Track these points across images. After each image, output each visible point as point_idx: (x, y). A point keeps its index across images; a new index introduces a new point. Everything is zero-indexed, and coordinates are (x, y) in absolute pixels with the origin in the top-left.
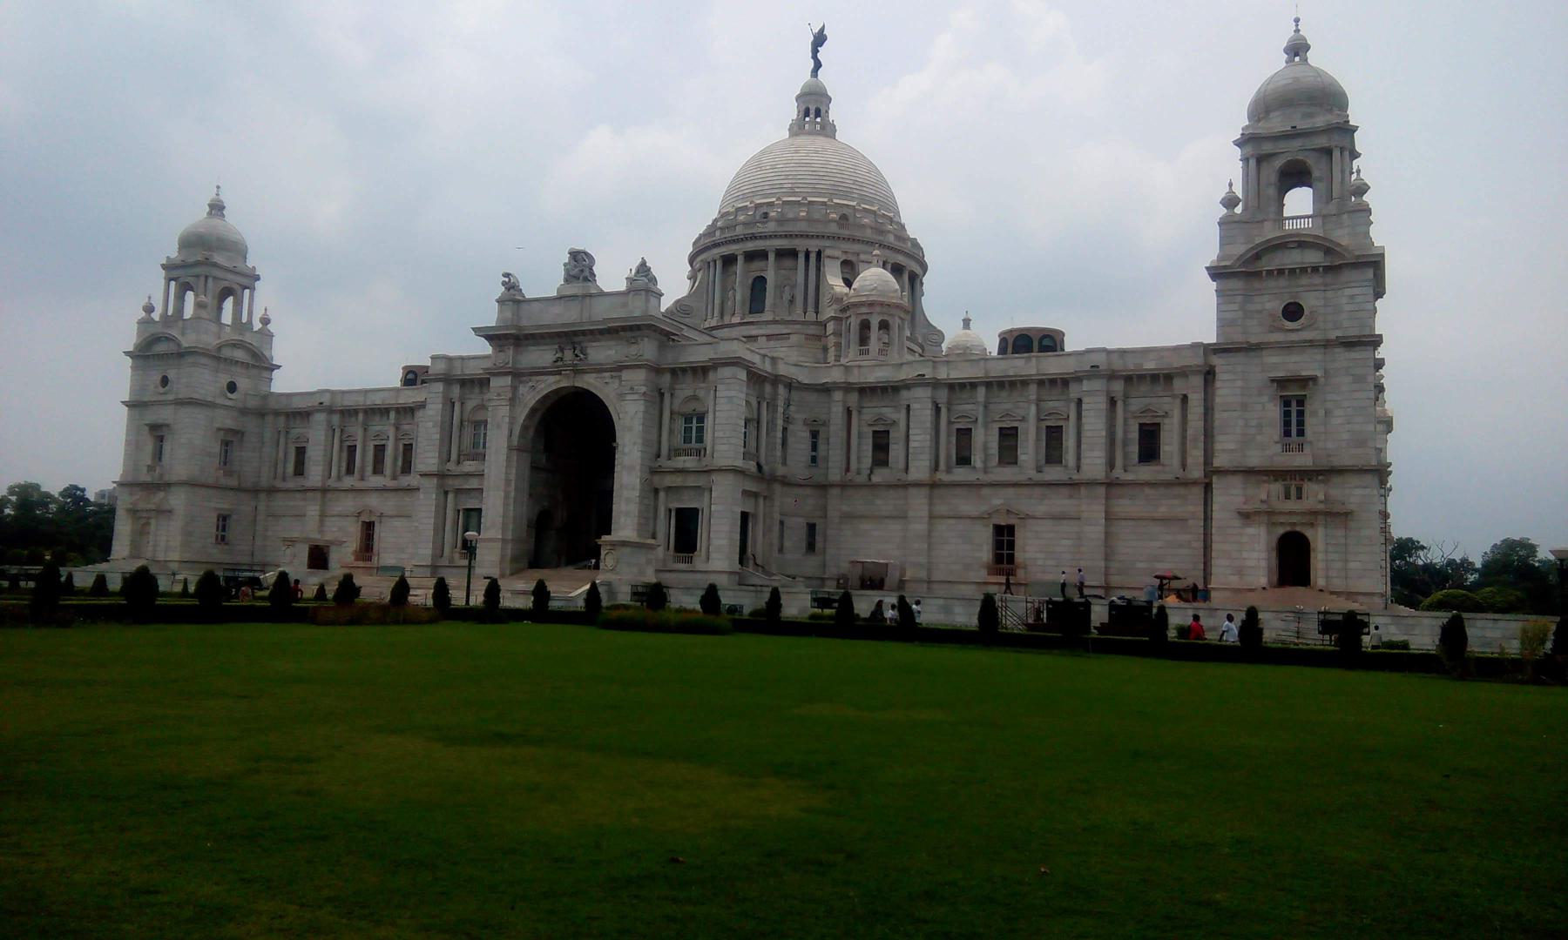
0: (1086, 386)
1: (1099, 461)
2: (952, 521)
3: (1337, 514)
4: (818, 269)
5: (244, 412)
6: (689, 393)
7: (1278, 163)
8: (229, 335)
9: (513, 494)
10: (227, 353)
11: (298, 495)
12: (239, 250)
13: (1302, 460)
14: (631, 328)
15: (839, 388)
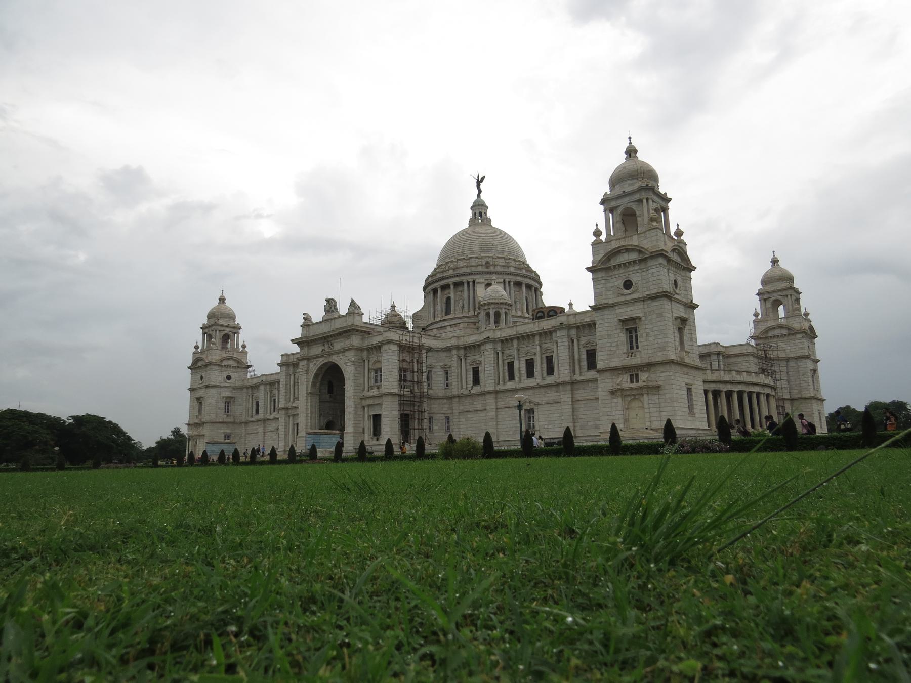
0: (559, 334)
1: (566, 372)
2: (507, 410)
3: (653, 387)
4: (474, 290)
5: (235, 388)
6: (375, 359)
7: (620, 211)
8: (229, 354)
9: (309, 415)
10: (225, 363)
11: (256, 423)
12: (232, 317)
13: (636, 360)
14: (346, 332)
15: (455, 348)
